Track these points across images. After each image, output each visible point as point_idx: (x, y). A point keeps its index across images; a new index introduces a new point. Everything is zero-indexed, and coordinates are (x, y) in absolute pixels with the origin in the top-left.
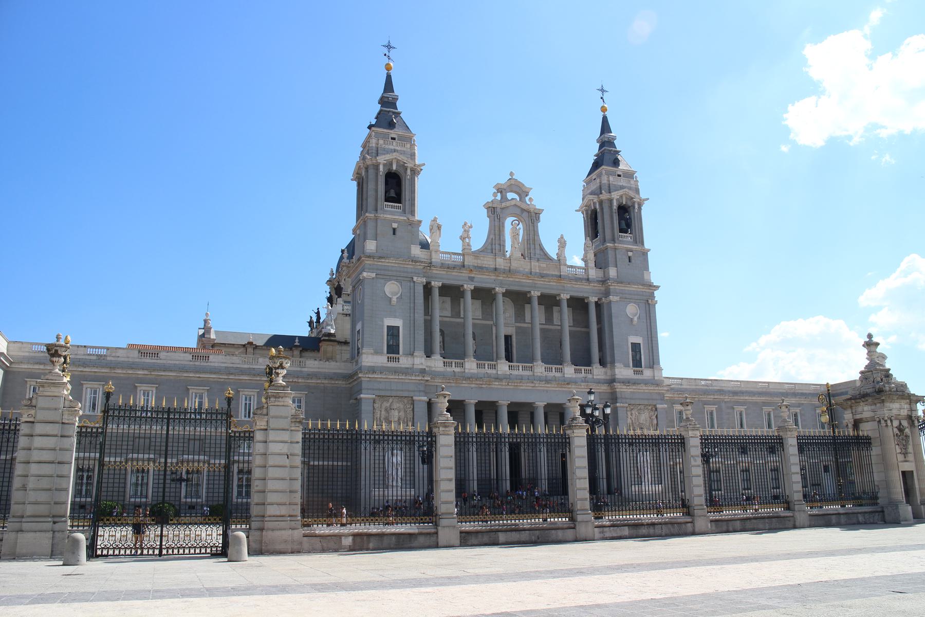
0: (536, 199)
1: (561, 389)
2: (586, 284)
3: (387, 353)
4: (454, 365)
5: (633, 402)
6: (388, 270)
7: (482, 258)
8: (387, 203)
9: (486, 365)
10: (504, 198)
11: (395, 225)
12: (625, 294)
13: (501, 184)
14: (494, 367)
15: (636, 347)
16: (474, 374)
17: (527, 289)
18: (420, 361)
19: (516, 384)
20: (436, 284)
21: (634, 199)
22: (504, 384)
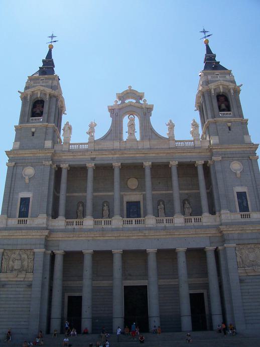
0: (149, 99)
3: (19, 217)
4: (75, 223)
5: (241, 242)
7: (103, 144)
8: (32, 118)
9: (103, 222)
10: (123, 102)
11: (33, 130)
12: (228, 154)
13: (120, 94)
18: (41, 220)
19: (127, 235)
22: (116, 235)
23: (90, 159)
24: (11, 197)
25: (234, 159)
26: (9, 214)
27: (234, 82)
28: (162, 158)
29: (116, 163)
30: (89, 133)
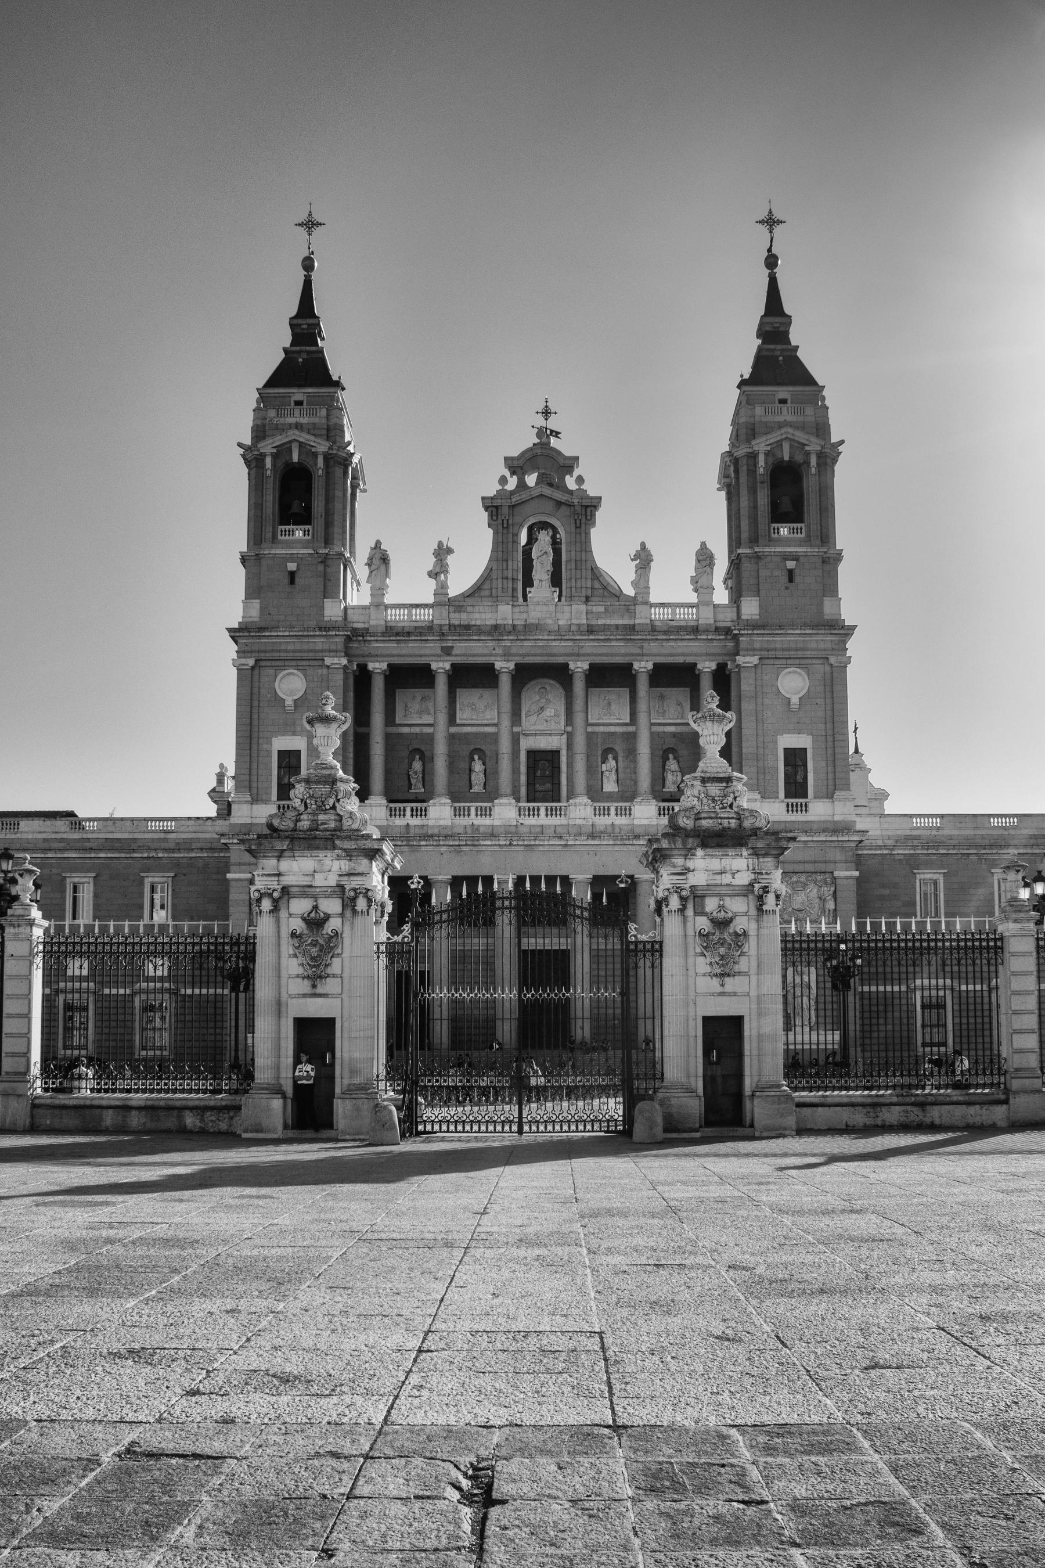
1: (624, 848)
2: (688, 637)
3: (279, 799)
6: (279, 651)
7: (469, 609)
8: (283, 527)
9: (473, 810)
10: (522, 485)
11: (292, 566)
12: (775, 649)
13: (512, 459)
14: (487, 812)
15: (795, 758)
16: (446, 827)
17: (561, 660)
20: (378, 667)
21: (807, 448)
22: (502, 843)
23: (439, 652)
24: (255, 747)
25: (789, 661)
26: (254, 791)
27: (822, 429)
28: (615, 651)
29: (504, 664)
30: (433, 574)
